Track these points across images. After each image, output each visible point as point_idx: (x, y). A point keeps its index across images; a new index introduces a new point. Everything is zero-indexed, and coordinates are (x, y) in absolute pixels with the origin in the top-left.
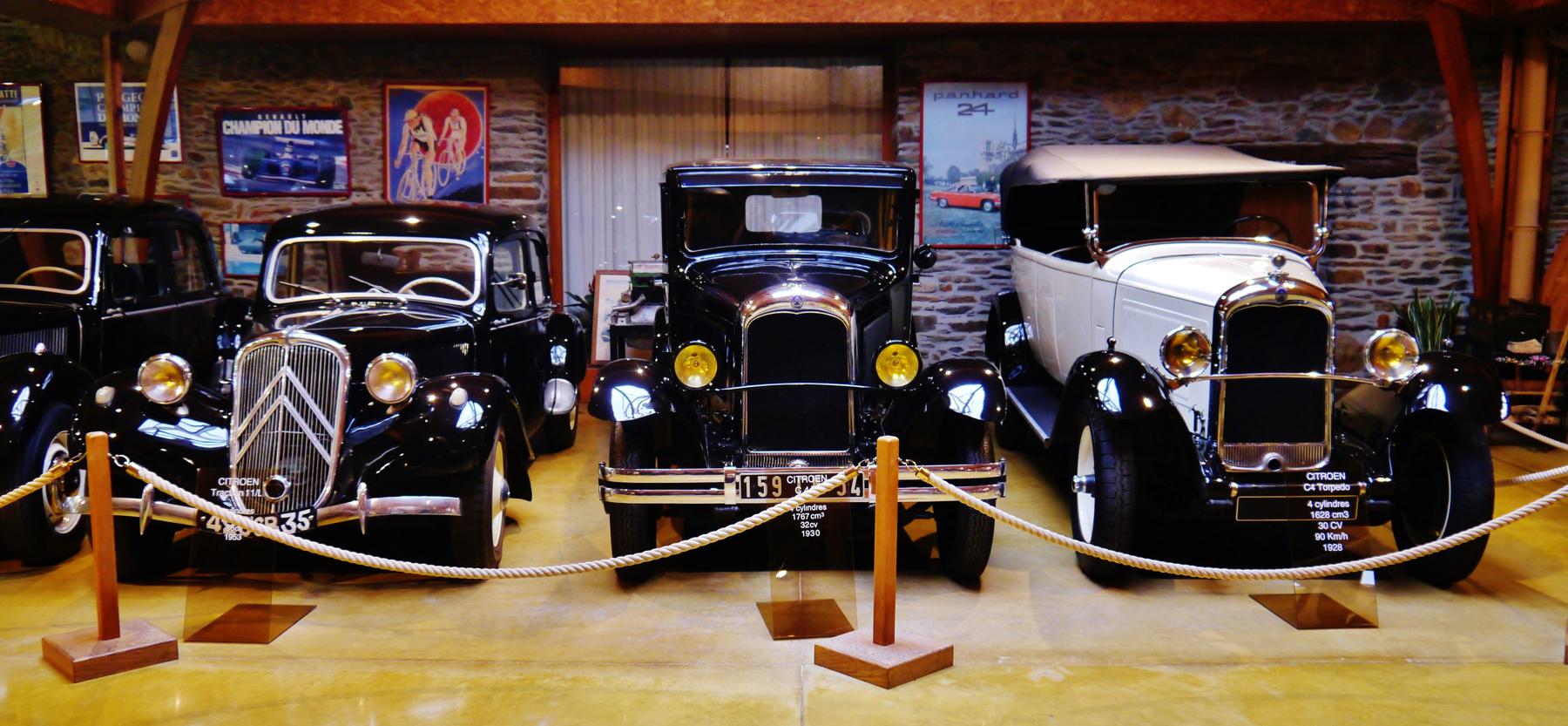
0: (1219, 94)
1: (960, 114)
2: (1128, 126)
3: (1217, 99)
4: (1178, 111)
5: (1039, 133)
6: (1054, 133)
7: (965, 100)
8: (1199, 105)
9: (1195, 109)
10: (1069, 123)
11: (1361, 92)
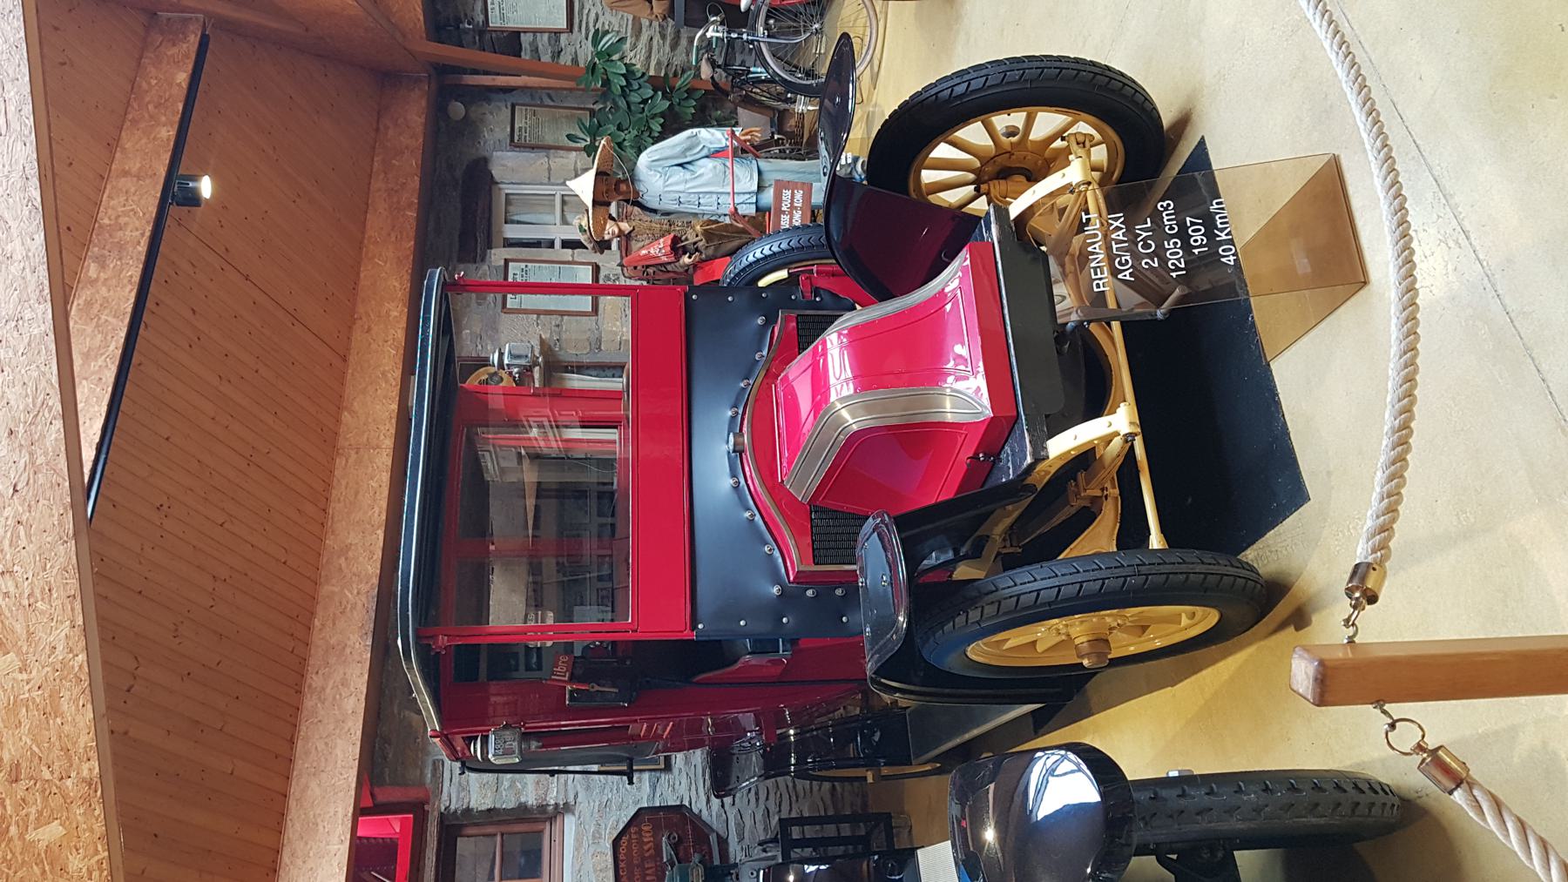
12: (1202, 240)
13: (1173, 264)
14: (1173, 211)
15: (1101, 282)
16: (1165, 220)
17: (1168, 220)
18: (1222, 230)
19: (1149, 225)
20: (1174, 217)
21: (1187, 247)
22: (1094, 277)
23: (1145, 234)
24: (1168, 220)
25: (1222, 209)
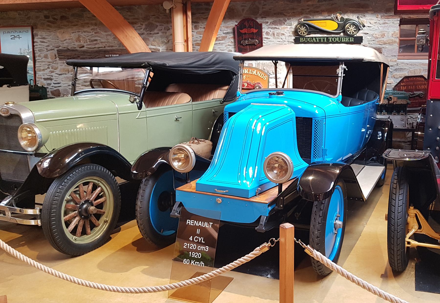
0: (92, 29)
1: (11, 39)
2: (65, 42)
3: (91, 31)
4: (79, 36)
5: (37, 45)
6: (42, 45)
7: (12, 34)
8: (85, 34)
9: (85, 35)
10: (46, 42)
11: (138, 28)
12: (193, 256)
13: (192, 245)
15: (189, 222)
17: (202, 248)
18: (194, 262)
19: (202, 242)
21: (192, 251)
22: (192, 221)
23: (200, 240)
25: (201, 265)
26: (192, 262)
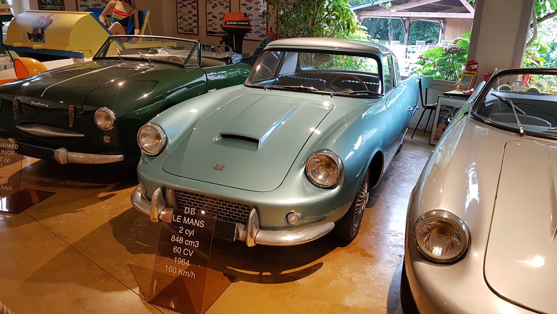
14: (194, 246)
16: (191, 241)
20: (191, 245)
24: (191, 243)
26: (179, 272)
